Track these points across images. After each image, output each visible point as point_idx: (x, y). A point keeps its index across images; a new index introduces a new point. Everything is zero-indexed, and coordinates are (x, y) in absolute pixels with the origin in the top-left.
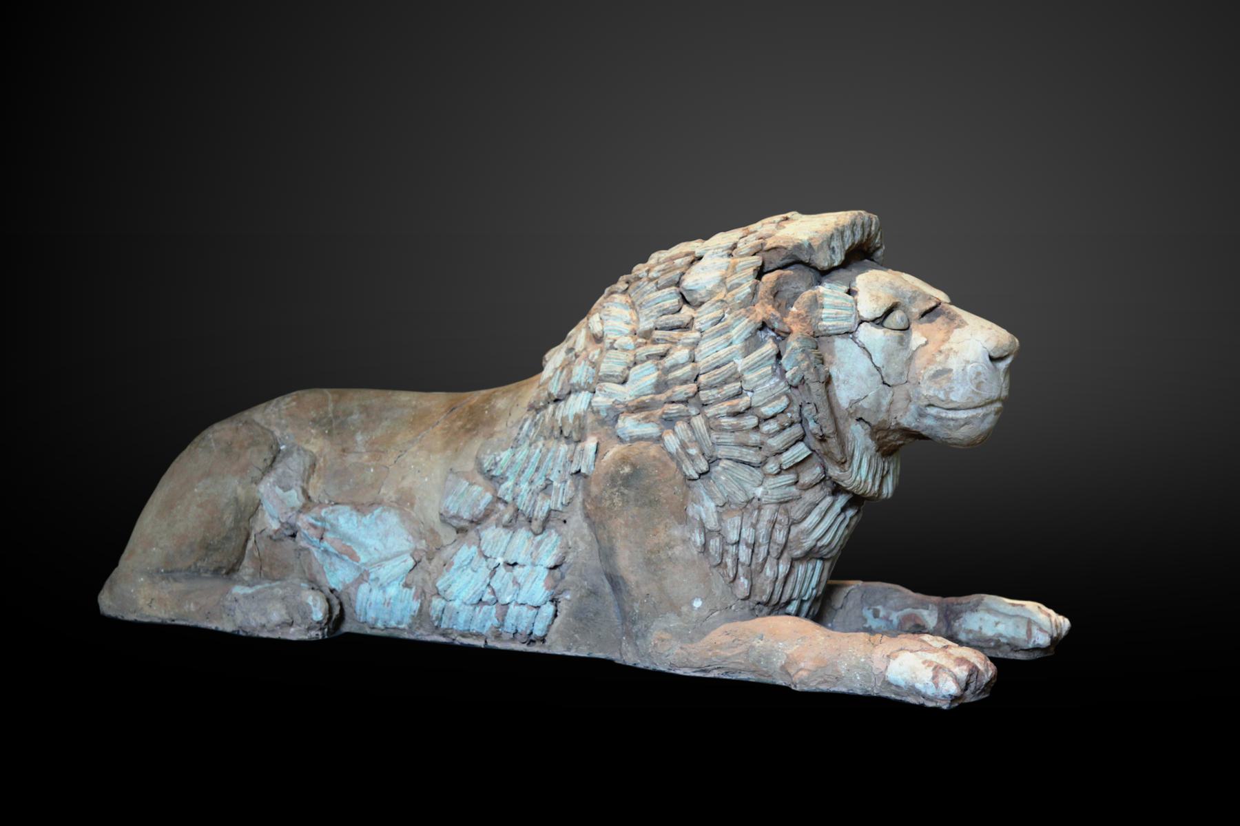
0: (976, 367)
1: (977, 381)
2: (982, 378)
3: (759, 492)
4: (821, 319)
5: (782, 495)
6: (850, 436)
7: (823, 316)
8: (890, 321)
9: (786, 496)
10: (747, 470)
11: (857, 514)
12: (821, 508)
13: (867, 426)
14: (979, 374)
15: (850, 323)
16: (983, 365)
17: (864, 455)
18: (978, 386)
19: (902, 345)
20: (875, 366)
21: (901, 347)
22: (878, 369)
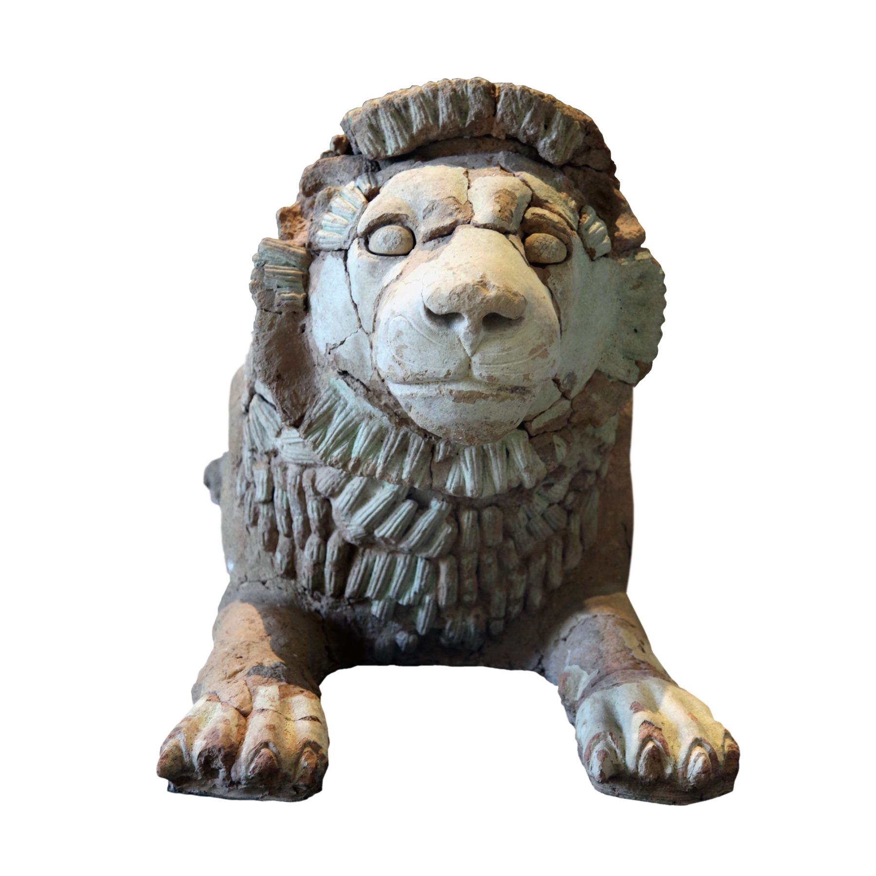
0: (398, 323)
1: (399, 343)
2: (405, 340)
3: (278, 443)
4: (321, 227)
5: (298, 455)
6: (324, 395)
7: (323, 222)
8: (378, 239)
9: (303, 457)
10: (266, 412)
11: (410, 504)
12: (353, 485)
13: (357, 384)
14: (399, 334)
15: (341, 237)
16: (411, 321)
17: (363, 424)
18: (399, 350)
19: (373, 276)
20: (353, 302)
21: (372, 279)
22: (356, 306)
